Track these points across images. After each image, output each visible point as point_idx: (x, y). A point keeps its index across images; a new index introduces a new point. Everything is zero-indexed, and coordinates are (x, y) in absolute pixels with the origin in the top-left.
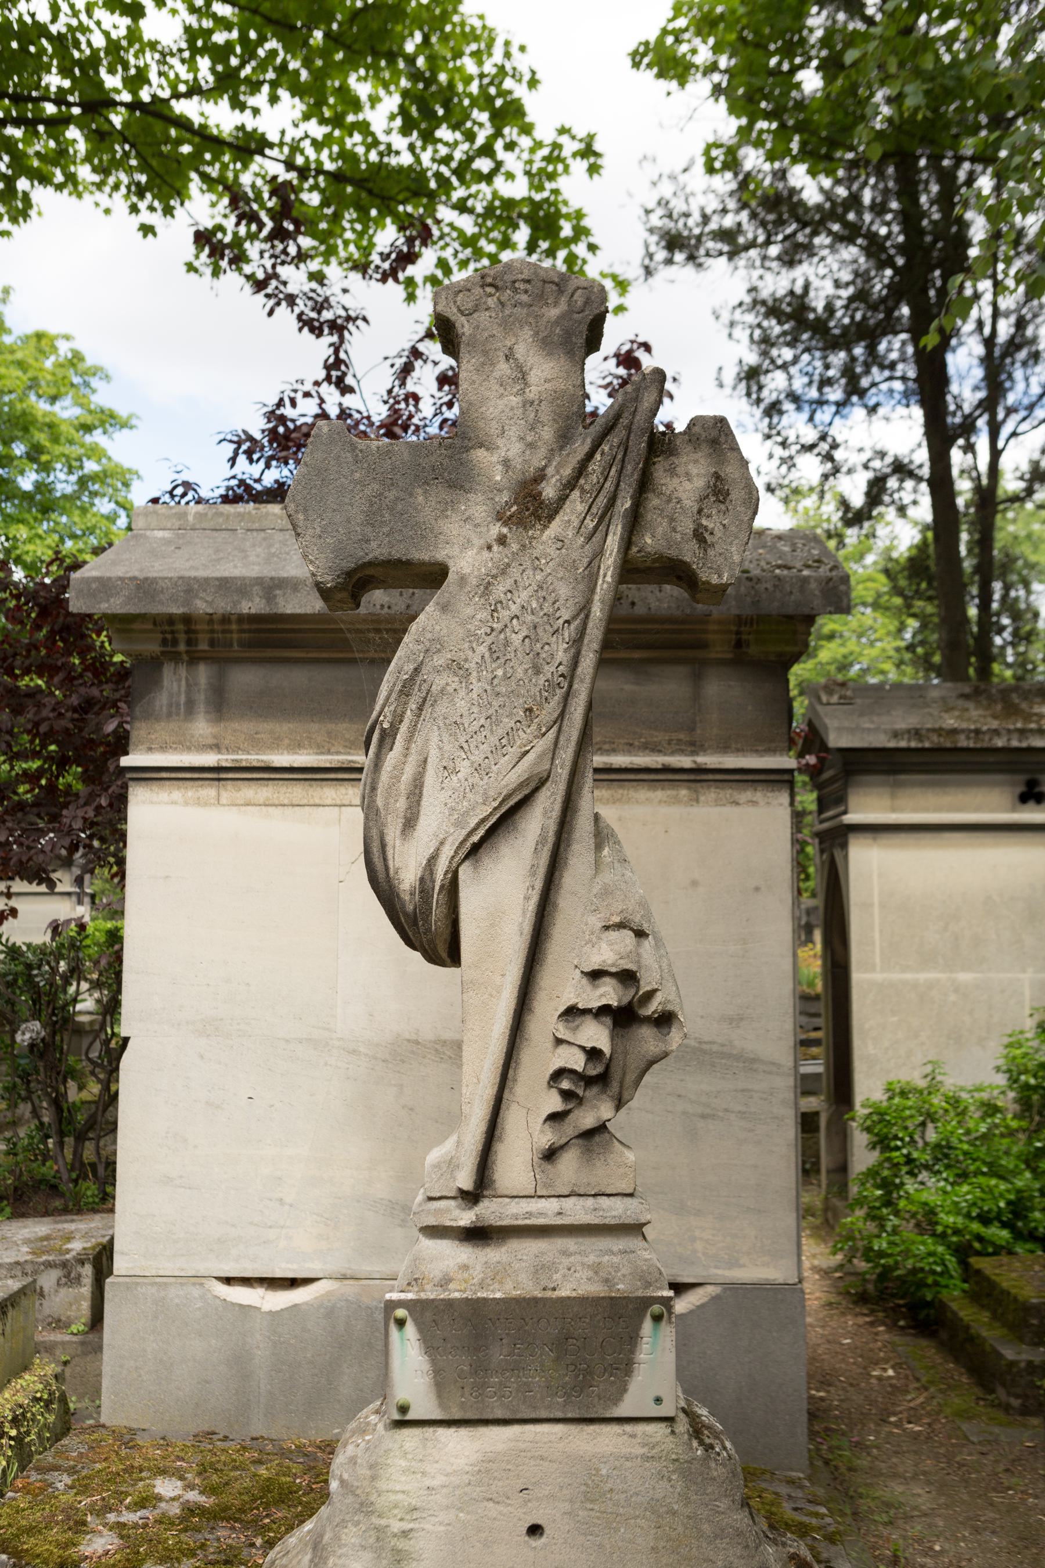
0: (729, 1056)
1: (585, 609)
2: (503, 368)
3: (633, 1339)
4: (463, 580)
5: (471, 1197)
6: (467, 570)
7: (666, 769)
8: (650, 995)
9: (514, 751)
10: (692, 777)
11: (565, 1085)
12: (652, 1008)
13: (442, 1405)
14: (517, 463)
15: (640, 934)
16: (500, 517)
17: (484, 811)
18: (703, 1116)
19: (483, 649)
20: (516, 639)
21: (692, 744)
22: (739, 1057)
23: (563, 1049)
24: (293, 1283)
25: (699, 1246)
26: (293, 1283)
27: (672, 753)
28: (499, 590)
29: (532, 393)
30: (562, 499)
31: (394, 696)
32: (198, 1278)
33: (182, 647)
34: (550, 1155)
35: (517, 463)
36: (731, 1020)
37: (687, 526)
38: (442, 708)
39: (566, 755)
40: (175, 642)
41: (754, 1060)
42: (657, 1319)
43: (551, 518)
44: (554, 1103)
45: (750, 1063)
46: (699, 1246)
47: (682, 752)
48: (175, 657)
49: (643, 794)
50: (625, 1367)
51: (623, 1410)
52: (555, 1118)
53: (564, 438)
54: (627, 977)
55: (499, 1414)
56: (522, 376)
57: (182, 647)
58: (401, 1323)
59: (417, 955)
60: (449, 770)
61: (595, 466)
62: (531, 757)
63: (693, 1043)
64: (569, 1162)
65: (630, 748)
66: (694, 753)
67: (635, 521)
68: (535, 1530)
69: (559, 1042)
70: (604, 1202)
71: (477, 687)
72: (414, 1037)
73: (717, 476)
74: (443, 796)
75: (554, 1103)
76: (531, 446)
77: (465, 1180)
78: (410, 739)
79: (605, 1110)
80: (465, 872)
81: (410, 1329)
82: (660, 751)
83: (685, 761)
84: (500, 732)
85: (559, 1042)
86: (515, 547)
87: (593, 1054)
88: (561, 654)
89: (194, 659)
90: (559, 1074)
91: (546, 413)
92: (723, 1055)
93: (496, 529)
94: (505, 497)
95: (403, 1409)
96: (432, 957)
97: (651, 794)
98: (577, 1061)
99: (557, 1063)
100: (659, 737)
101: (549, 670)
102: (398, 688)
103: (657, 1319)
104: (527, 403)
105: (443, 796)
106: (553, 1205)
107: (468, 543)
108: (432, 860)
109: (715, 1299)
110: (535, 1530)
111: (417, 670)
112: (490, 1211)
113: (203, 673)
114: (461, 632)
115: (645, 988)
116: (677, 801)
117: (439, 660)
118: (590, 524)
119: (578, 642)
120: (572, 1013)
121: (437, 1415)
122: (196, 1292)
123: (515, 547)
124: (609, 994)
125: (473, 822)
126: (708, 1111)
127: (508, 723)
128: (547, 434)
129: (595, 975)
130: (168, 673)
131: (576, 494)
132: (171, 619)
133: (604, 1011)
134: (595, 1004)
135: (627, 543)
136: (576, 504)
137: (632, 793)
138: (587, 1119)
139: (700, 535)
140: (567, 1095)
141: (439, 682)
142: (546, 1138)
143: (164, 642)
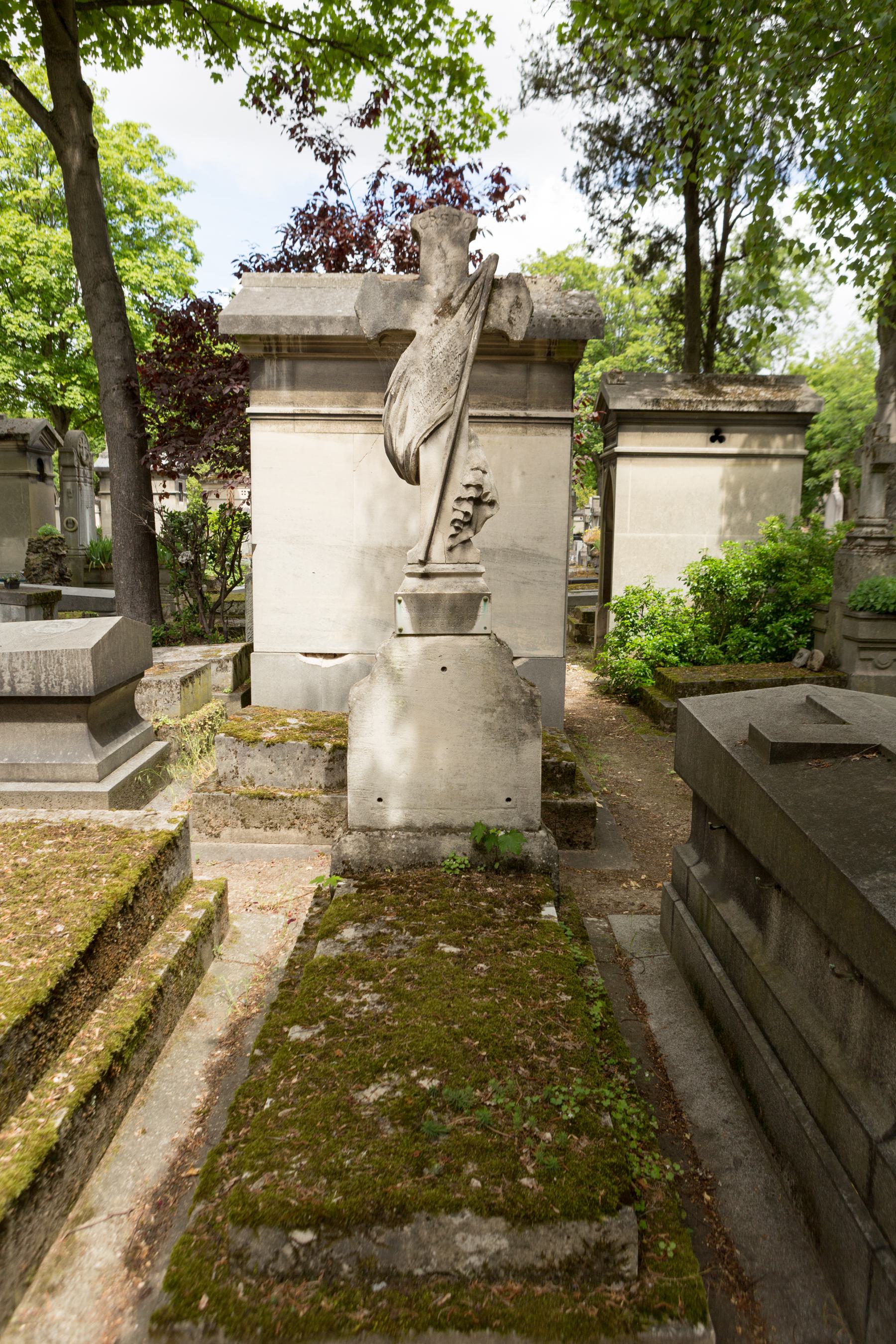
0: (537, 555)
3: (477, 607)
4: (421, 338)
5: (423, 563)
7: (512, 417)
8: (487, 494)
9: (440, 404)
11: (456, 525)
14: (442, 291)
15: (484, 472)
22: (541, 556)
24: (335, 656)
25: (519, 641)
26: (335, 656)
28: (435, 342)
29: (448, 262)
30: (459, 306)
32: (293, 653)
33: (274, 352)
34: (451, 549)
37: (505, 317)
38: (413, 387)
39: (459, 405)
40: (270, 349)
41: (548, 558)
42: (486, 601)
43: (454, 314)
44: (453, 531)
45: (546, 559)
46: (519, 641)
47: (519, 408)
48: (271, 357)
49: (501, 429)
50: (475, 617)
51: (473, 631)
54: (479, 487)
56: (444, 255)
57: (274, 352)
58: (400, 601)
59: (404, 481)
61: (471, 293)
64: (457, 551)
65: (494, 406)
66: (526, 409)
67: (486, 315)
68: (444, 669)
69: (454, 510)
75: (453, 531)
77: (422, 558)
79: (470, 534)
80: (421, 448)
83: (521, 413)
85: (454, 510)
87: (466, 514)
88: (458, 367)
89: (279, 359)
90: (454, 521)
92: (533, 555)
94: (438, 305)
95: (401, 630)
96: (410, 482)
98: (461, 516)
99: (454, 517)
100: (509, 401)
101: (453, 373)
103: (486, 601)
106: (452, 566)
109: (526, 664)
110: (444, 669)
112: (430, 568)
113: (285, 365)
115: (485, 491)
116: (516, 433)
118: (469, 316)
120: (459, 500)
121: (412, 632)
122: (292, 659)
124: (472, 493)
129: (468, 486)
130: (267, 364)
132: (268, 337)
133: (470, 499)
135: (483, 324)
136: (463, 310)
138: (463, 537)
139: (510, 321)
140: (457, 528)
141: (412, 377)
142: (450, 543)
143: (265, 349)
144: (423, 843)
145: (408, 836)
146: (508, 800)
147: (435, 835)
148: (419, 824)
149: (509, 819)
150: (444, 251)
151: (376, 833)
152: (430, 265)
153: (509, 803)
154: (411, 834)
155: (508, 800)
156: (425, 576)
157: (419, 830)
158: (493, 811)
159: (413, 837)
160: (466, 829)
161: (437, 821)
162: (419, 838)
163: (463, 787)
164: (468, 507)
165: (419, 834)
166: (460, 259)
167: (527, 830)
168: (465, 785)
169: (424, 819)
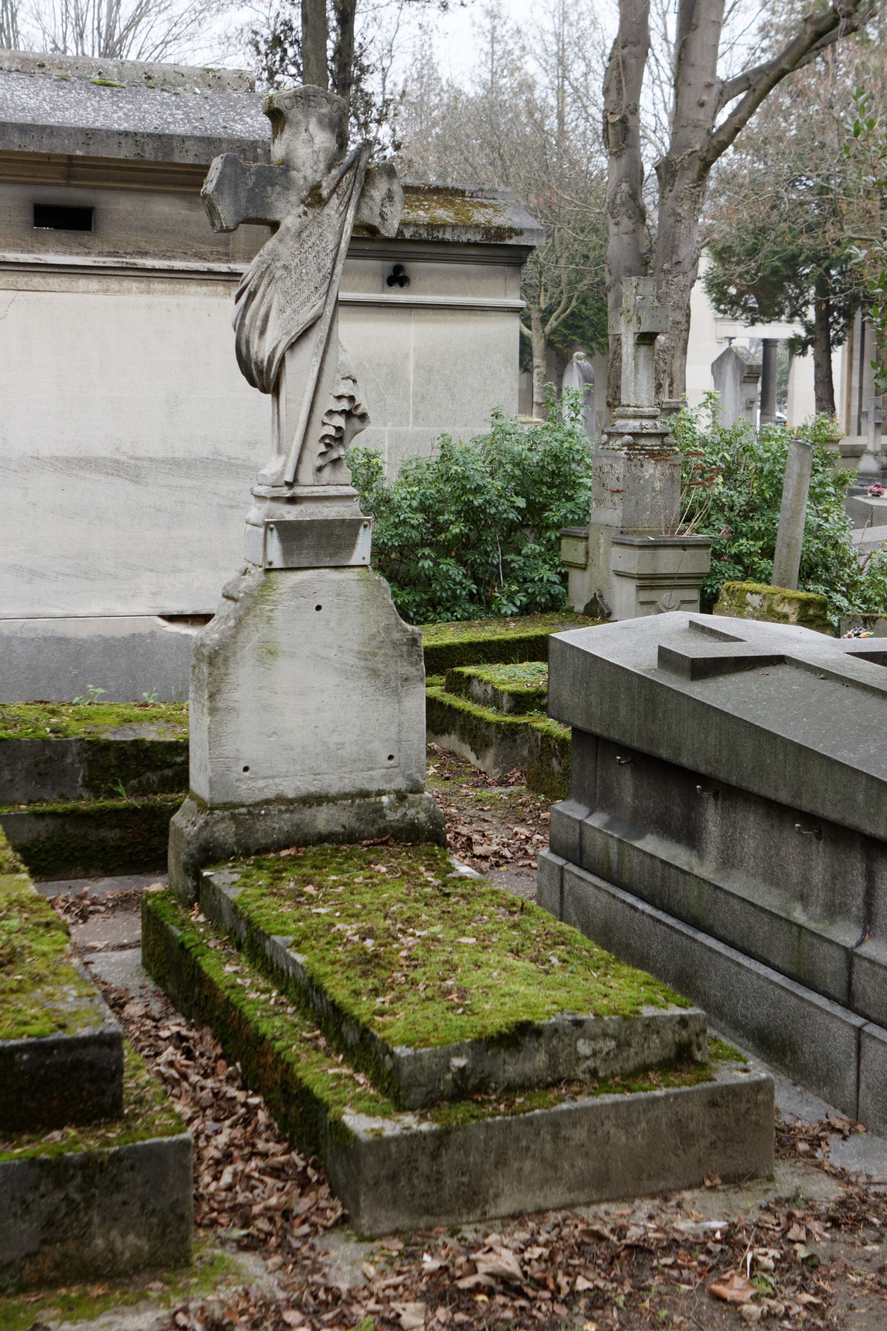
1: (338, 245)
2: (304, 135)
3: (356, 534)
4: (288, 229)
6: (290, 226)
7: (210, 272)
10: (227, 278)
11: (327, 441)
12: (359, 411)
13: (285, 562)
14: (310, 179)
15: (354, 381)
16: (303, 202)
17: (296, 330)
18: (231, 507)
19: (297, 260)
20: (310, 257)
21: (227, 255)
23: (326, 427)
27: (214, 261)
28: (304, 235)
31: (256, 277)
34: (320, 469)
35: (310, 179)
36: (249, 444)
37: (377, 211)
38: (280, 284)
42: (365, 526)
44: (323, 448)
47: (219, 260)
49: (192, 288)
50: (352, 546)
51: (352, 562)
52: (322, 454)
53: (329, 168)
54: (352, 399)
55: (306, 565)
56: (311, 140)
58: (272, 529)
60: (282, 311)
61: (344, 184)
62: (316, 307)
63: (225, 459)
64: (327, 472)
65: (185, 256)
66: (228, 261)
67: (358, 209)
68: (319, 608)
69: (324, 424)
70: (340, 487)
71: (295, 276)
72: (36, 455)
73: (389, 190)
74: (279, 322)
75: (323, 448)
76: (316, 171)
78: (263, 297)
80: (287, 356)
81: (275, 533)
82: (200, 258)
83: (223, 267)
84: (304, 296)
85: (324, 424)
86: (311, 217)
87: (338, 429)
88: (329, 265)
91: (322, 157)
93: (302, 208)
94: (305, 193)
95: (270, 563)
97: (198, 289)
98: (332, 432)
99: (324, 433)
100: (206, 248)
101: (324, 271)
102: (259, 273)
103: (365, 526)
104: (314, 152)
105: (279, 322)
106: (321, 489)
107: (289, 213)
108: (275, 350)
110: (319, 608)
111: (268, 267)
112: (299, 491)
114: (288, 253)
116: (216, 294)
117: (278, 264)
118: (342, 209)
119: (335, 261)
120: (330, 413)
123: (311, 217)
124: (345, 405)
125: (293, 334)
126: (234, 503)
127: (307, 293)
128: (322, 166)
129: (340, 398)
131: (335, 195)
133: (342, 412)
134: (340, 409)
136: (335, 201)
137: (186, 288)
138: (334, 455)
139: (382, 215)
141: (278, 274)
142: (320, 462)
144: (296, 817)
145: (280, 811)
146: (391, 757)
147: (310, 807)
148: (291, 795)
149: (391, 781)
150: (311, 136)
151: (243, 810)
152: (296, 149)
153: (392, 762)
154: (283, 808)
155: (391, 757)
156: (292, 500)
157: (291, 802)
158: (374, 773)
159: (287, 811)
160: (345, 796)
161: (312, 789)
162: (292, 812)
163: (341, 746)
164: (340, 421)
165: (292, 807)
166: (327, 145)
167: (411, 792)
168: (343, 744)
169: (297, 788)
